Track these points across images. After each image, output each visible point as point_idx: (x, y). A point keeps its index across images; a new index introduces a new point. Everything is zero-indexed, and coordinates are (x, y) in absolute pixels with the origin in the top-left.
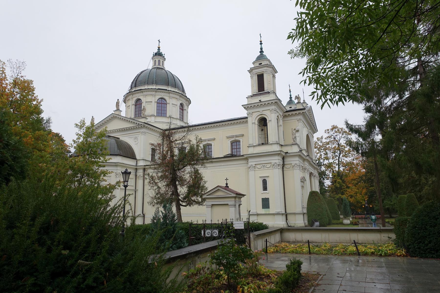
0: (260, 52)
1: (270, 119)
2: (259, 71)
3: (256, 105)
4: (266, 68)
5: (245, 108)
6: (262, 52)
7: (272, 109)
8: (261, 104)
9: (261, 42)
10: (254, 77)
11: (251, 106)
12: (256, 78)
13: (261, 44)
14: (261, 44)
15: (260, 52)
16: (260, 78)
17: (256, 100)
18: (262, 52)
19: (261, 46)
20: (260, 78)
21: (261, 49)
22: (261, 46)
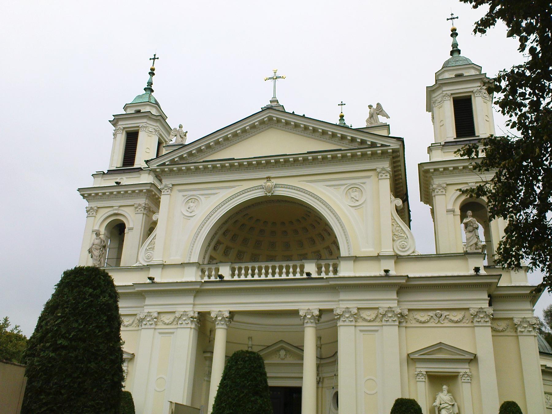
0: (145, 89)
1: (131, 226)
2: (131, 124)
3: (107, 191)
4: (145, 120)
5: (83, 195)
6: (149, 89)
7: (140, 205)
8: (119, 192)
9: (153, 70)
10: (119, 136)
11: (111, 193)
12: (122, 139)
13: (152, 74)
14: (152, 74)
15: (145, 89)
16: (132, 139)
17: (110, 182)
18: (149, 89)
19: (151, 79)
20: (132, 139)
21: (150, 84)
22: (151, 79)
